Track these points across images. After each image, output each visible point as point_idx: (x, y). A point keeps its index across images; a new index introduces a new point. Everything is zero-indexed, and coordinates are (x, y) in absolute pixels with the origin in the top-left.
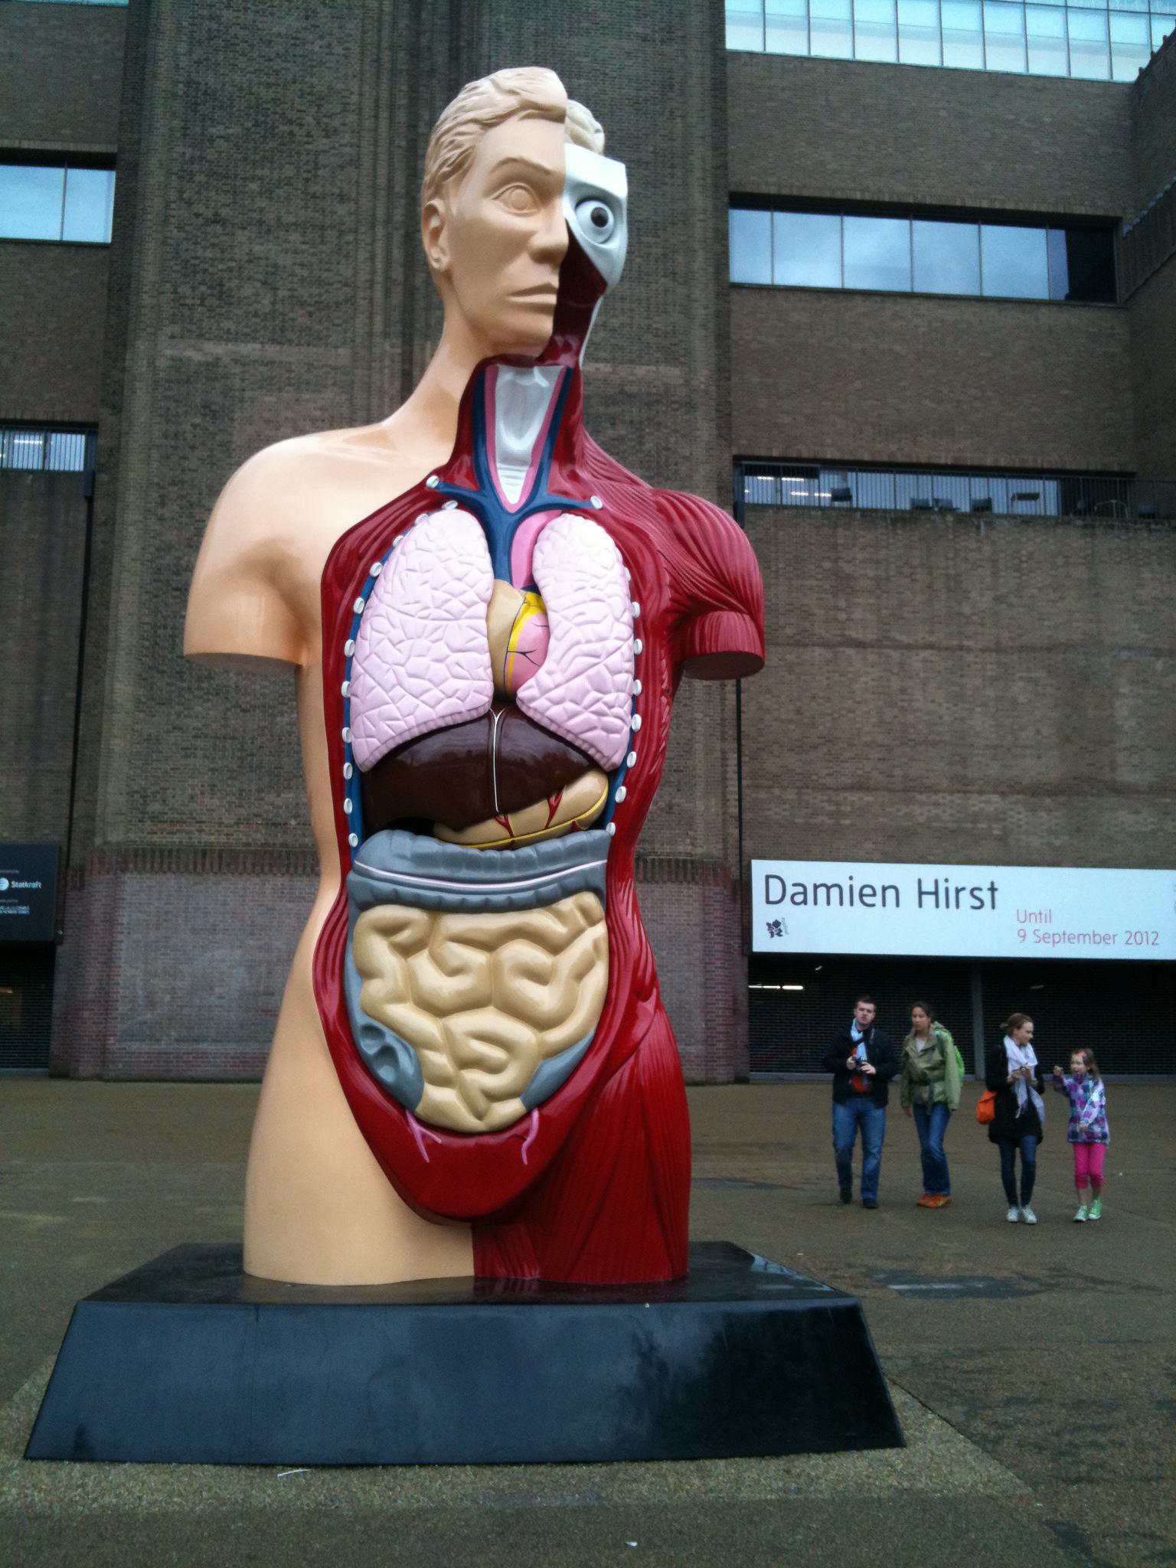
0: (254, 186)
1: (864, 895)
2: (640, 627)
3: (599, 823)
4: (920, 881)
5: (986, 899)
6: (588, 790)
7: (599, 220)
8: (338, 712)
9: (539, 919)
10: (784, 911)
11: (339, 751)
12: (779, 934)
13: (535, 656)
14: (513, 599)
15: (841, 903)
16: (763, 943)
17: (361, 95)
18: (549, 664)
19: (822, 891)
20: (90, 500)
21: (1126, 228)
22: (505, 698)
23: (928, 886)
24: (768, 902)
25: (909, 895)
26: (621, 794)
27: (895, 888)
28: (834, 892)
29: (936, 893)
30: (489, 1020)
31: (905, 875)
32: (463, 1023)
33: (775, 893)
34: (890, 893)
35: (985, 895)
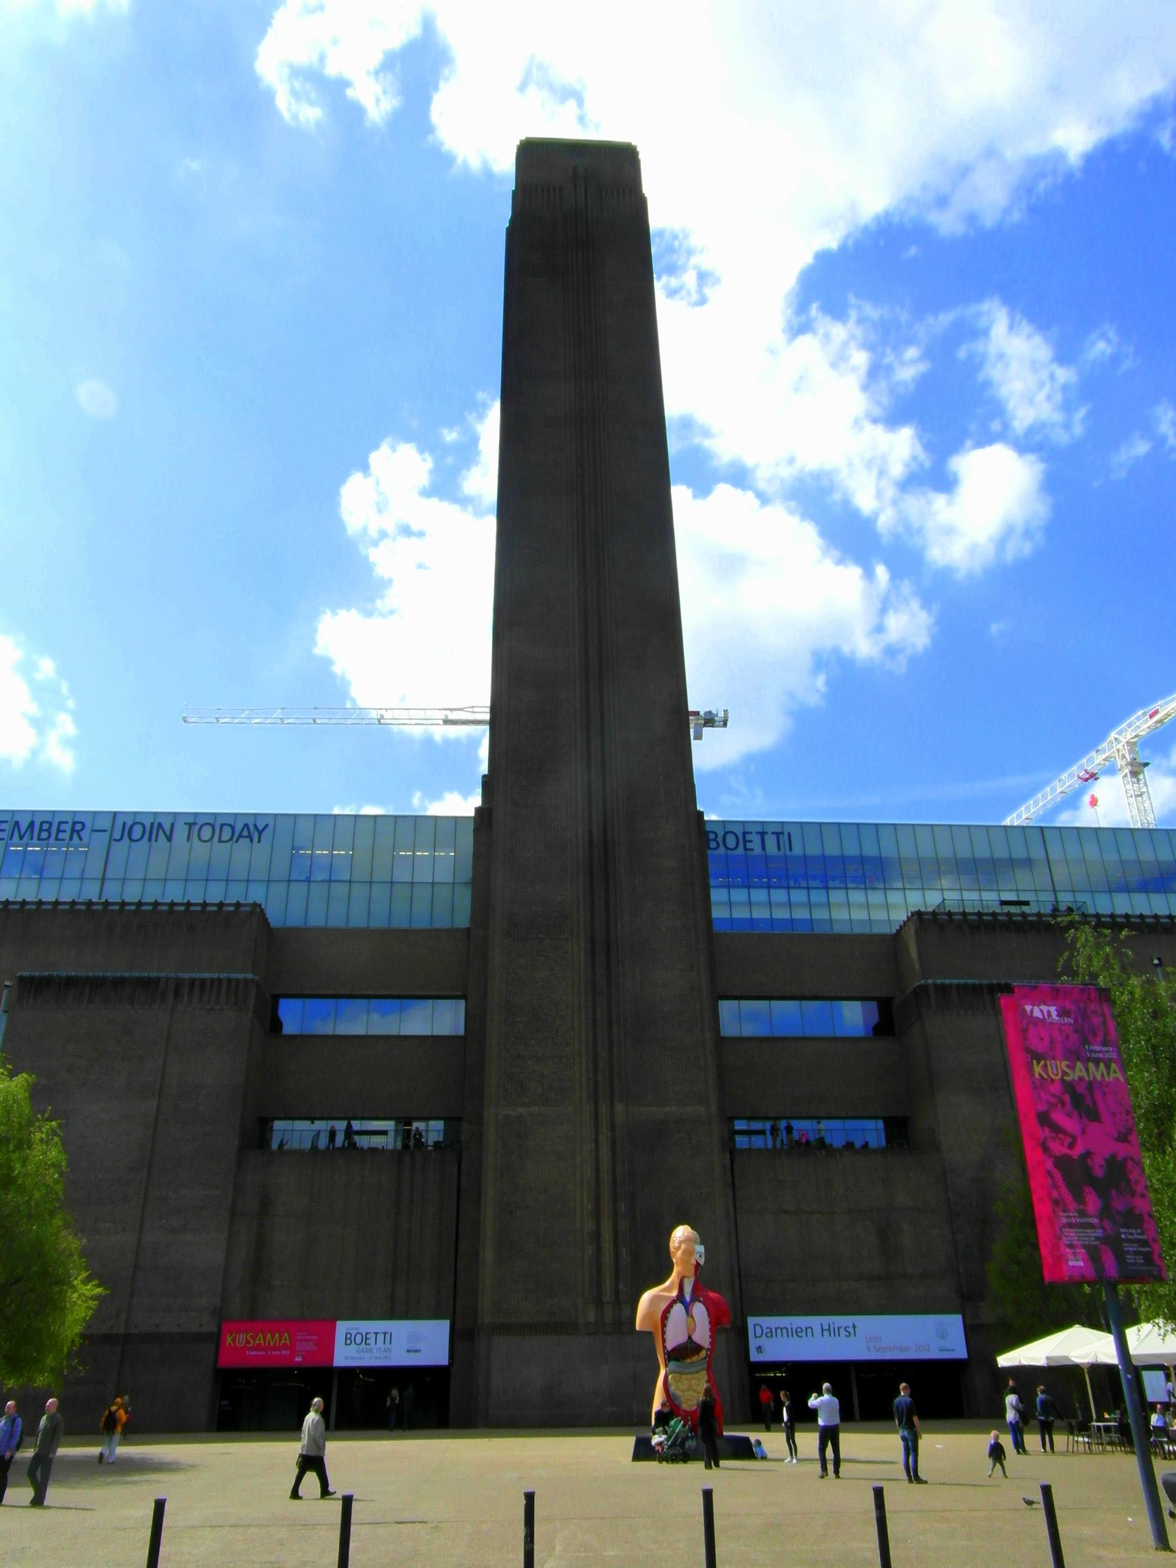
0: (533, 1042)
1: (797, 1332)
2: (710, 1323)
3: (705, 1358)
4: (822, 1325)
5: (851, 1331)
6: (703, 1354)
7: (700, 1256)
8: (664, 1340)
9: (696, 1375)
10: (763, 1341)
11: (664, 1347)
12: (761, 1352)
13: (694, 1330)
14: (690, 1319)
15: (788, 1336)
16: (754, 1357)
17: (573, 1001)
18: (696, 1332)
19: (779, 1331)
20: (459, 1164)
21: (896, 1002)
22: (690, 1338)
23: (826, 1327)
24: (756, 1337)
25: (817, 1331)
26: (709, 1353)
27: (811, 1328)
28: (784, 1331)
29: (829, 1330)
30: (691, 1392)
31: (814, 1321)
32: (686, 1393)
33: (759, 1332)
34: (809, 1330)
35: (851, 1330)
